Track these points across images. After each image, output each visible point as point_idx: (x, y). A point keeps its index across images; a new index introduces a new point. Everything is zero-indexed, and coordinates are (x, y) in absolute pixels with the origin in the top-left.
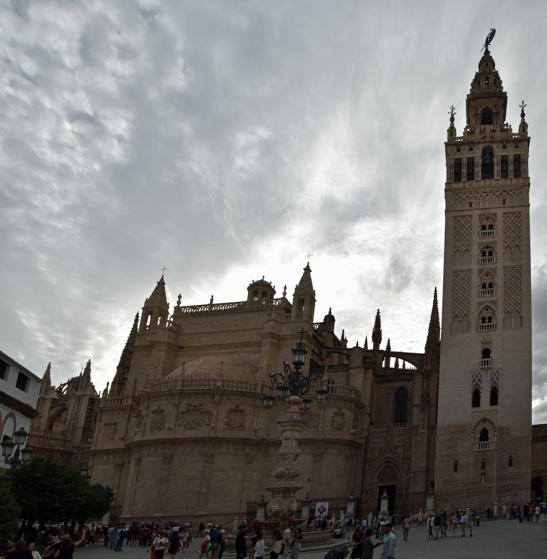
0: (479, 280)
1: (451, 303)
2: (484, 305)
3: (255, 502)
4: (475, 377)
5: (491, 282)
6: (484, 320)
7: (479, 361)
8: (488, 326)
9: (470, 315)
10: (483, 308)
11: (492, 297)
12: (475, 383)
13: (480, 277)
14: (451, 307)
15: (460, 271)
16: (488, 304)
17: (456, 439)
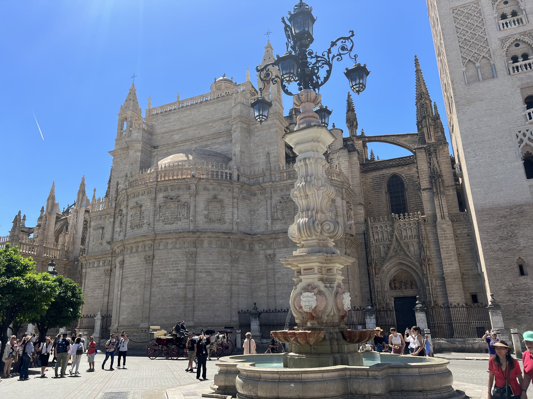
0: (495, 10)
1: (459, 48)
2: (511, 40)
3: (246, 312)
4: (521, 136)
5: (513, 10)
6: (515, 59)
7: (523, 114)
8: (525, 65)
9: (492, 56)
10: (510, 43)
11: (521, 28)
12: (524, 144)
13: (495, 7)
14: (460, 52)
15: (462, 6)
16: (517, 37)
17: (511, 225)
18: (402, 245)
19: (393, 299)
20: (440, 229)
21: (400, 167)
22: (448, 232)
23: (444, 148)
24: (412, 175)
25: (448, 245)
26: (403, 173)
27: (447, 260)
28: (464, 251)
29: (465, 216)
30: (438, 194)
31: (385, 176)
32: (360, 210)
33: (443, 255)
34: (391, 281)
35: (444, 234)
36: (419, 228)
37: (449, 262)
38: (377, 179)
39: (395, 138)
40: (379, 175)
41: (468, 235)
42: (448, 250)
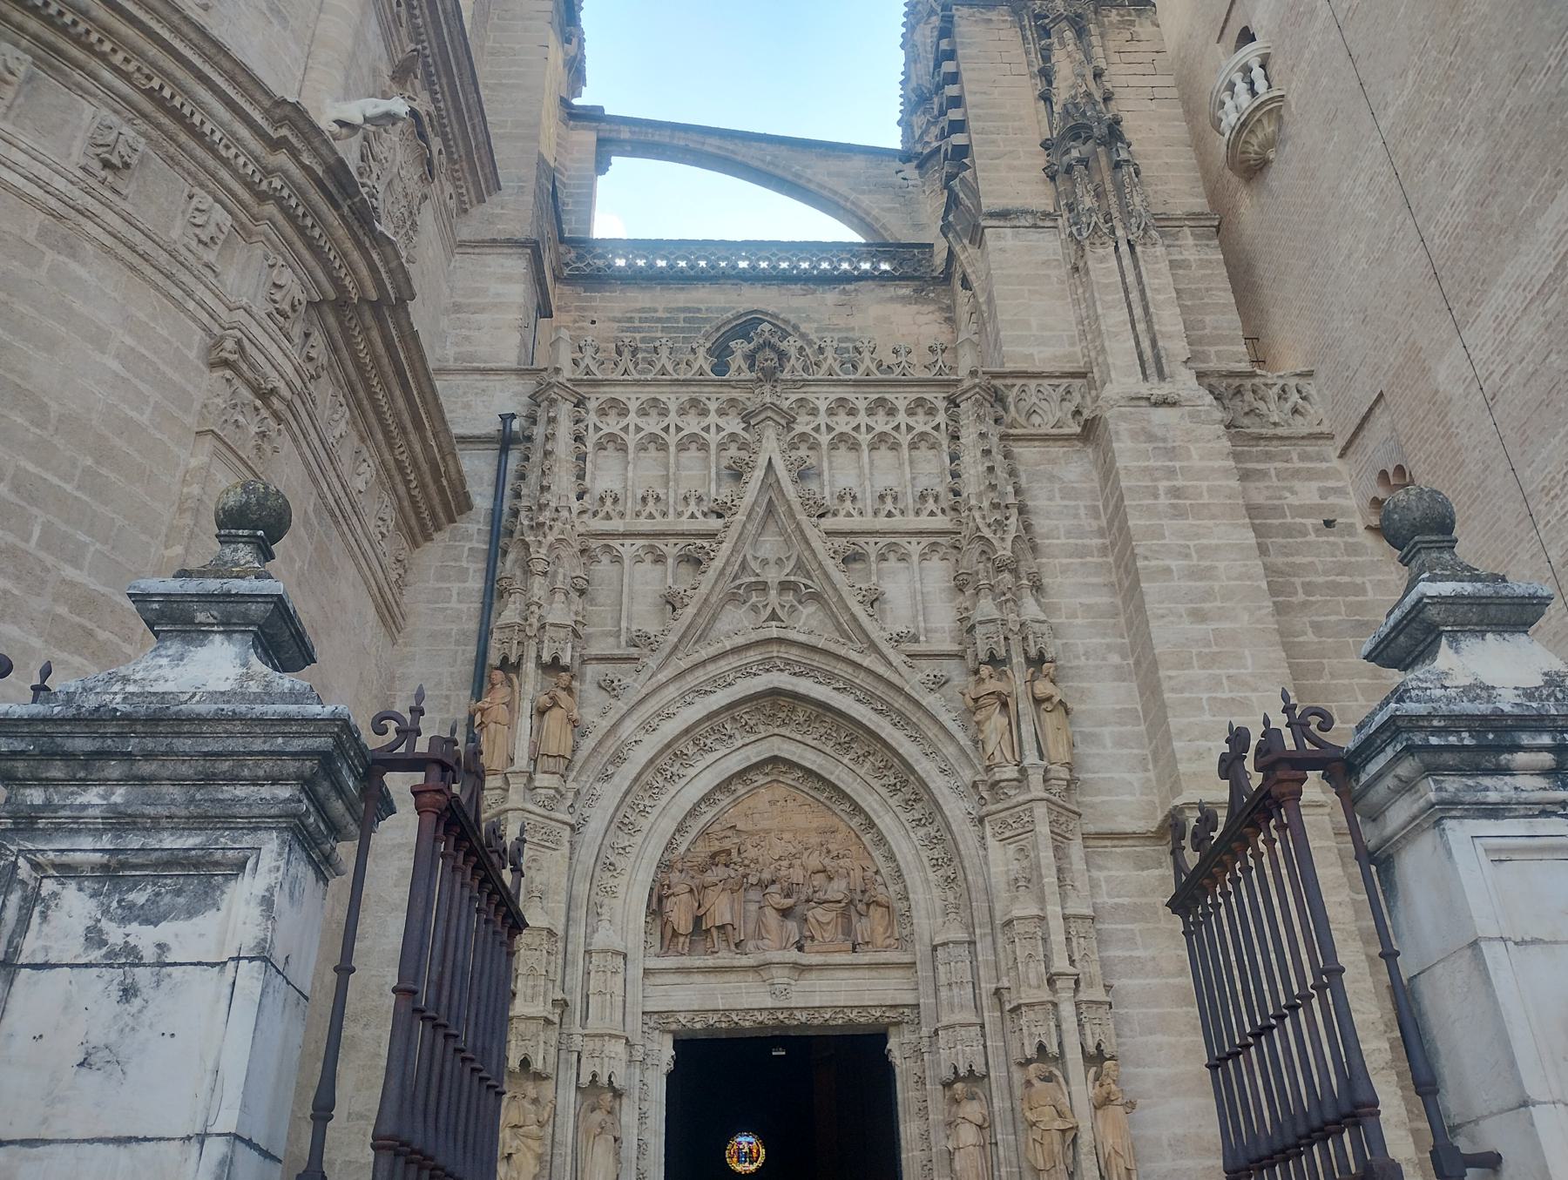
18: (817, 544)
19: (665, 1053)
20: (1134, 436)
21: (797, 288)
22: (1196, 462)
23: (1132, 23)
24: (857, 334)
25: (1202, 551)
26: (809, 319)
27: (1196, 672)
28: (1310, 637)
29: (1295, 397)
30: (1108, 218)
31: (706, 320)
32: (506, 279)
33: (1165, 634)
34: (665, 866)
35: (1171, 473)
36: (955, 437)
37: (1217, 683)
38: (650, 329)
39: (784, 151)
40: (667, 310)
41: (1329, 524)
42: (1209, 595)
